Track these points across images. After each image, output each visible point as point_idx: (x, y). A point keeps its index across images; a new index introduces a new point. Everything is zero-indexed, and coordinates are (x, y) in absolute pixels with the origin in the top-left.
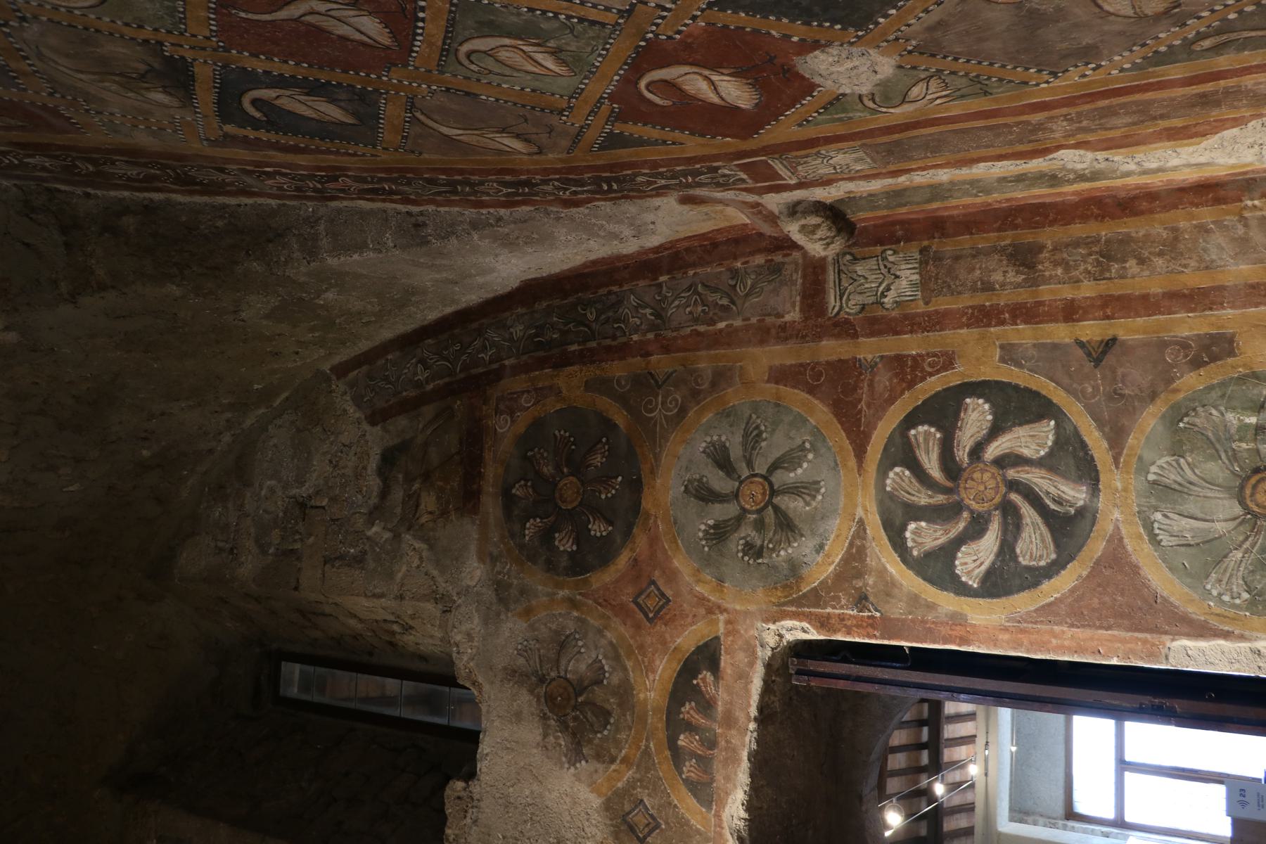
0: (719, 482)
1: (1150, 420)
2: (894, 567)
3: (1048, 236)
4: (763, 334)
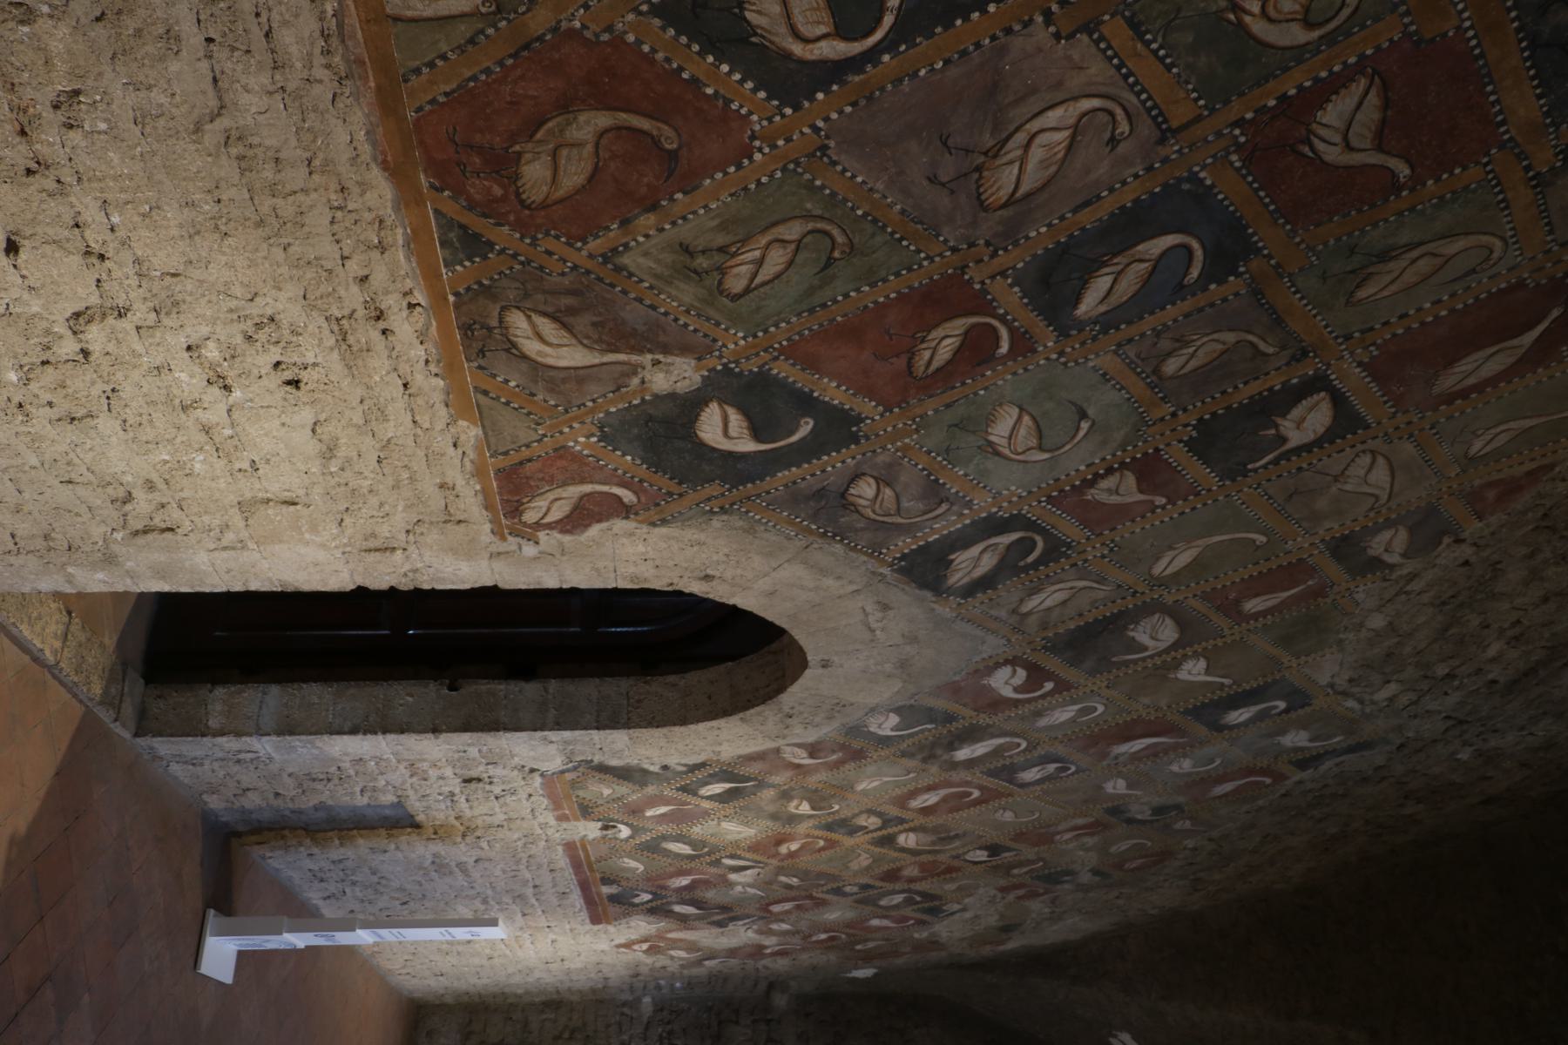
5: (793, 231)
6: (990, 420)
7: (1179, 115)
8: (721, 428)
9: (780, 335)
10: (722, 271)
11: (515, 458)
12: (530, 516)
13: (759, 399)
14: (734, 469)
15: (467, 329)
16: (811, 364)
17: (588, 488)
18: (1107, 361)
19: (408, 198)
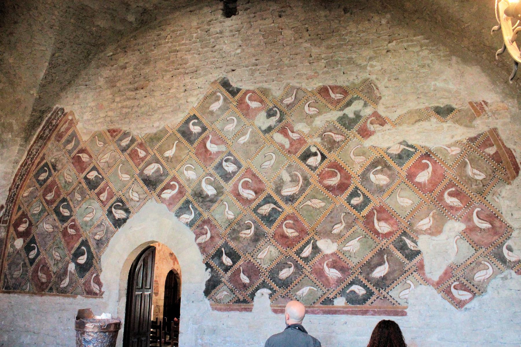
5: (54, 252)
7: (46, 214)
8: (82, 260)
9: (67, 252)
10: (57, 260)
11: (84, 291)
12: (98, 292)
13: (78, 254)
14: (91, 257)
15: (62, 293)
16: (72, 248)
17: (92, 281)
18: (77, 209)
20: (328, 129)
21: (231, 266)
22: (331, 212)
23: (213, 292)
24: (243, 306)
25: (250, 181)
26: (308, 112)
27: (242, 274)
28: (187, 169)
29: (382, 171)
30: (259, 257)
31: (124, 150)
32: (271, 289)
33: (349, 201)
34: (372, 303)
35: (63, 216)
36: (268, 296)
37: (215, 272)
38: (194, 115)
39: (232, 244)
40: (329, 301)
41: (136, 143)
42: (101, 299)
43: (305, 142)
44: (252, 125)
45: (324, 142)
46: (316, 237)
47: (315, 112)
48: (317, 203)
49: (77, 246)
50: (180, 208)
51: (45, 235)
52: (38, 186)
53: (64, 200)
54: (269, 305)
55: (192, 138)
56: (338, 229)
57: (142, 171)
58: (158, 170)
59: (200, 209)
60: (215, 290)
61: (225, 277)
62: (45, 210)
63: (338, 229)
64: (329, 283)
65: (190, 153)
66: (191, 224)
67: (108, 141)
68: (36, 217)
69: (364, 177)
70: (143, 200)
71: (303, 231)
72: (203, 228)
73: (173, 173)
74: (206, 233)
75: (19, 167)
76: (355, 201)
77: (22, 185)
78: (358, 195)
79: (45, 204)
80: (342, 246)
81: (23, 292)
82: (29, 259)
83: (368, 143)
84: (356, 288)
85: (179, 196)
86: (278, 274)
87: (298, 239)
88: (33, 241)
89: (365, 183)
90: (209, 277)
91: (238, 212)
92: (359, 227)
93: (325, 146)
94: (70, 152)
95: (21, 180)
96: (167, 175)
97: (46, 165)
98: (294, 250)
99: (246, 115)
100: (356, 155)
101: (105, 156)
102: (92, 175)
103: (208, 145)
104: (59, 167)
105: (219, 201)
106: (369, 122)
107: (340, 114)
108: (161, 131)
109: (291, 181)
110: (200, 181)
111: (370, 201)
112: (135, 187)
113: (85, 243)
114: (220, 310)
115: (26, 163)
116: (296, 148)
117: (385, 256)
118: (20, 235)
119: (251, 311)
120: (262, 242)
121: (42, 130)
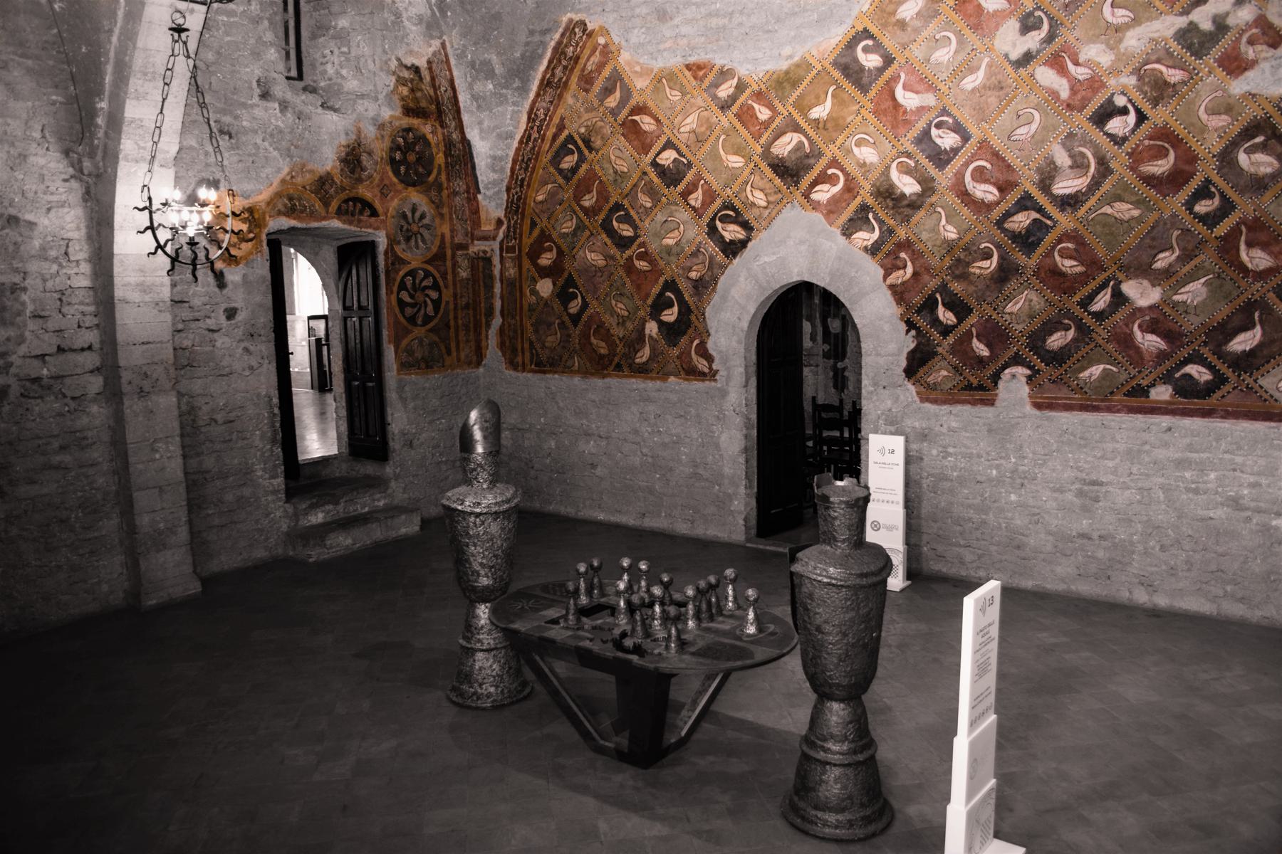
0: (417, 215)
1: (436, 339)
2: (402, 273)
3: (471, 312)
4: (452, 231)
5: (614, 302)
6: (668, 246)
7: (588, 233)
8: (670, 315)
9: (639, 303)
12: (706, 370)
13: (660, 305)
14: (685, 310)
16: (648, 295)
19: (609, 375)
20: (1153, 58)
21: (955, 327)
22: (1153, 228)
23: (921, 371)
24: (978, 395)
25: (989, 166)
26: (1110, 19)
27: (975, 340)
28: (858, 144)
29: (1263, 148)
30: (1008, 310)
31: (725, 106)
32: (1029, 367)
33: (1189, 205)
34: (1223, 397)
35: (621, 237)
36: (1024, 380)
37: (924, 336)
38: (865, 30)
39: (956, 287)
40: (1142, 392)
41: (747, 93)
42: (713, 384)
43: (1103, 85)
44: (990, 49)
45: (1144, 84)
46: (1121, 276)
47: (1127, 19)
48: (1124, 210)
49: (656, 290)
50: (851, 220)
51: (592, 272)
52: (561, 180)
53: (618, 207)
54: (1026, 395)
55: (865, 80)
56: (1164, 260)
57: (767, 148)
58: (800, 144)
59: (892, 222)
60: (925, 368)
61: (945, 346)
62: (586, 227)
63: (1164, 260)
64: (1142, 359)
65: (862, 111)
66: (873, 250)
67: (688, 88)
68: (569, 239)
69: (1226, 158)
70: (776, 206)
71: (1093, 265)
72: (898, 257)
73: (830, 151)
74: (905, 267)
75: (515, 144)
76: (1202, 207)
77: (530, 179)
78: (1210, 196)
79: (582, 215)
80: (1170, 293)
81: (567, 370)
82: (569, 315)
83: (1238, 87)
84: (1192, 369)
85: (847, 196)
86: (1044, 341)
87: (1083, 279)
88: (570, 282)
89: (1225, 170)
90: (912, 346)
91: (965, 227)
92: (1206, 258)
93: (1146, 93)
94: (614, 112)
95: (526, 169)
96: (820, 155)
97: (570, 139)
98: (1077, 298)
99: (976, 28)
100: (1212, 112)
101: (689, 120)
102: (668, 157)
103: (900, 93)
104: (597, 142)
105: (926, 205)
106: (1244, 39)
107: (1182, 22)
108: (798, 66)
109: (1071, 167)
110: (888, 168)
111: (1234, 208)
112: (756, 179)
113: (671, 285)
114: (935, 402)
115: (530, 136)
116: (1083, 98)
117: (1257, 314)
118: (545, 272)
119: (993, 404)
120: (1013, 284)
121: (548, 67)
